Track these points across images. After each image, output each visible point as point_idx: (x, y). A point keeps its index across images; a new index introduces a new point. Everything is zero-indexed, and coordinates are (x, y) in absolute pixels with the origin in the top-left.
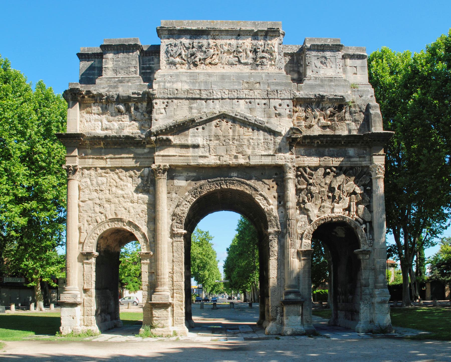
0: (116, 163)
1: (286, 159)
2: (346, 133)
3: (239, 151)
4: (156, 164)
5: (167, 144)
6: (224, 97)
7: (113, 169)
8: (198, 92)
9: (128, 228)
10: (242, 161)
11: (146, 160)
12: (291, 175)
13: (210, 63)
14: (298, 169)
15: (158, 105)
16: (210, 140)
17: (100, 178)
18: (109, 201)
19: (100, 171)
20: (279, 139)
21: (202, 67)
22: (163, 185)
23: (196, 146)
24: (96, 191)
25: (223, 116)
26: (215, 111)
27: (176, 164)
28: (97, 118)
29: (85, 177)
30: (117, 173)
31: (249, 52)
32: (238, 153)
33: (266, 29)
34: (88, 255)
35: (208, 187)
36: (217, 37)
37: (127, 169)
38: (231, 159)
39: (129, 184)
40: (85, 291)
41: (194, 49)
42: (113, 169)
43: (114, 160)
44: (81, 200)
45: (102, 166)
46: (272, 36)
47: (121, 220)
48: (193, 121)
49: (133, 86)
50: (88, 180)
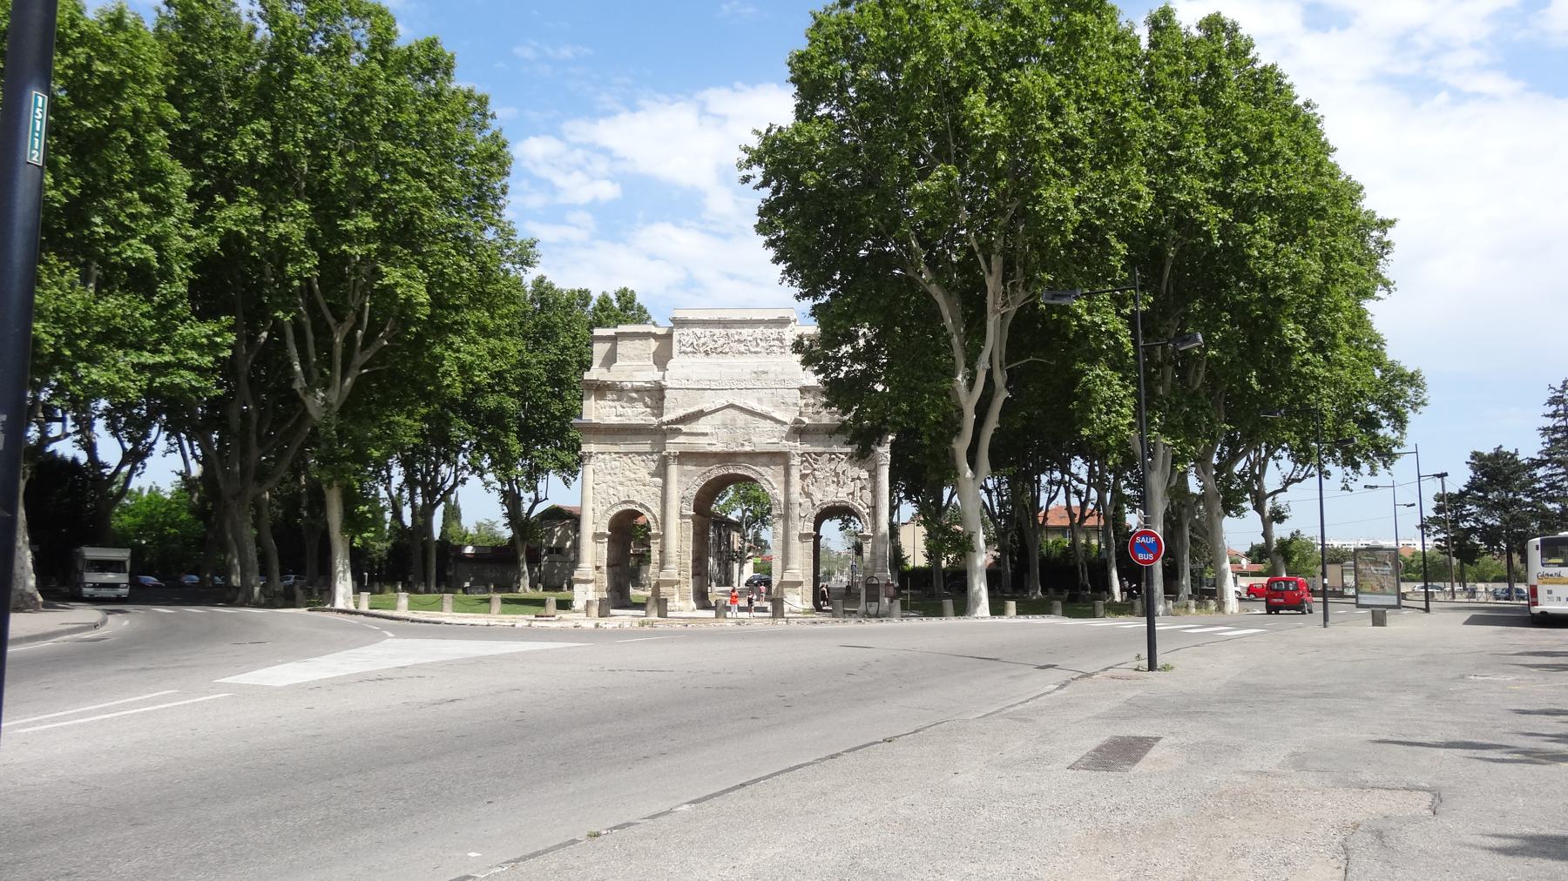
5: (678, 432)
7: (626, 454)
10: (747, 448)
12: (796, 461)
18: (621, 484)
20: (786, 428)
22: (673, 469)
23: (705, 434)
25: (732, 406)
34: (602, 535)
35: (717, 471)
37: (639, 454)
39: (642, 470)
40: (597, 568)
42: (626, 454)
49: (647, 374)
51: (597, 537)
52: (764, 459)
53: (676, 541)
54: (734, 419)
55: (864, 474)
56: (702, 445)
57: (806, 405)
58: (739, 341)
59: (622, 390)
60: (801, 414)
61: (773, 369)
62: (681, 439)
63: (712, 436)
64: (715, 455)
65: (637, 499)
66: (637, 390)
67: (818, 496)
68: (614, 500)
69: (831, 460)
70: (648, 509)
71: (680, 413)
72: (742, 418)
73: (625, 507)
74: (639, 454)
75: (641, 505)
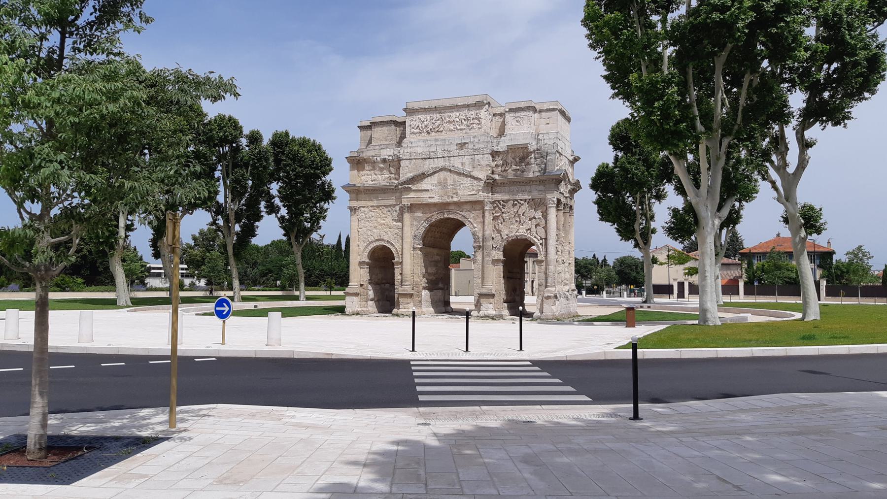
1: (483, 196)
2: (531, 175)
7: (378, 207)
9: (387, 245)
10: (455, 199)
14: (494, 202)
42: (378, 207)
47: (383, 240)
48: (423, 174)
51: (361, 263)
52: (468, 207)
53: (411, 267)
54: (445, 179)
55: (539, 215)
56: (426, 198)
57: (497, 166)
58: (450, 122)
60: (493, 173)
62: (412, 195)
63: (431, 191)
64: (435, 205)
66: (384, 161)
67: (505, 232)
69: (514, 205)
70: (392, 245)
71: (410, 175)
73: (379, 243)
74: (386, 206)
75: (388, 242)
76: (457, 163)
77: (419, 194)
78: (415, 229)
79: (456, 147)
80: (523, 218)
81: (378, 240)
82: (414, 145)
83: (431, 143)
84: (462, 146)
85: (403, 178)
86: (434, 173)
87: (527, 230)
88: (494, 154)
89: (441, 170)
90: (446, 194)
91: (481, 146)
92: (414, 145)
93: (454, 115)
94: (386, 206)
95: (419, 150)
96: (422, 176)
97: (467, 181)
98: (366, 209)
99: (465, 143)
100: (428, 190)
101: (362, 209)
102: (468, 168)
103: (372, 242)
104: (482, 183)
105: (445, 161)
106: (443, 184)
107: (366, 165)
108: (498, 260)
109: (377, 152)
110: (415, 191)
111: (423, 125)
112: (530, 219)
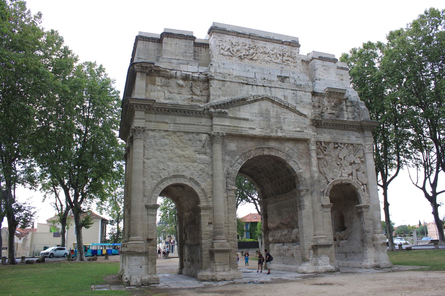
0: (178, 128)
3: (278, 126)
4: (214, 131)
6: (264, 85)
8: (246, 79)
10: (280, 134)
11: (204, 127)
13: (251, 59)
15: (214, 84)
16: (256, 117)
17: (163, 140)
19: (163, 134)
21: (245, 61)
24: (159, 150)
26: (260, 94)
27: (230, 132)
28: (160, 89)
29: (150, 138)
30: (178, 137)
31: (278, 56)
32: (278, 128)
33: (290, 41)
36: (255, 41)
38: (272, 132)
41: (239, 47)
42: (174, 132)
43: (176, 125)
44: (145, 157)
45: (166, 129)
46: (293, 46)
48: (244, 99)
50: (152, 140)
54: (267, 110)
55: (358, 161)
56: (246, 128)
59: (171, 77)
61: (292, 75)
62: (227, 122)
65: (187, 174)
66: (186, 78)
67: (330, 176)
68: (165, 174)
70: (197, 183)
71: (226, 99)
72: (273, 110)
74: (187, 133)
75: (191, 179)
76: (278, 94)
77: (235, 123)
78: (227, 165)
79: (276, 79)
80: (345, 163)
81: (175, 176)
82: (226, 66)
83: (248, 68)
84: (283, 79)
85: (214, 101)
86: (255, 101)
87: (349, 175)
88: (314, 94)
89: (262, 99)
90: (269, 126)
91: (303, 83)
92: (226, 66)
93: (269, 46)
94: (187, 133)
95: (235, 73)
96: (243, 101)
97: (291, 116)
98: (157, 134)
99: (286, 77)
100: (247, 120)
101: (151, 133)
102: (291, 102)
103: (166, 179)
104: (308, 122)
105: (265, 90)
106: (265, 115)
107: (158, 79)
108: (327, 207)
109: (174, 66)
110: (231, 118)
111: (235, 49)
112: (351, 164)
